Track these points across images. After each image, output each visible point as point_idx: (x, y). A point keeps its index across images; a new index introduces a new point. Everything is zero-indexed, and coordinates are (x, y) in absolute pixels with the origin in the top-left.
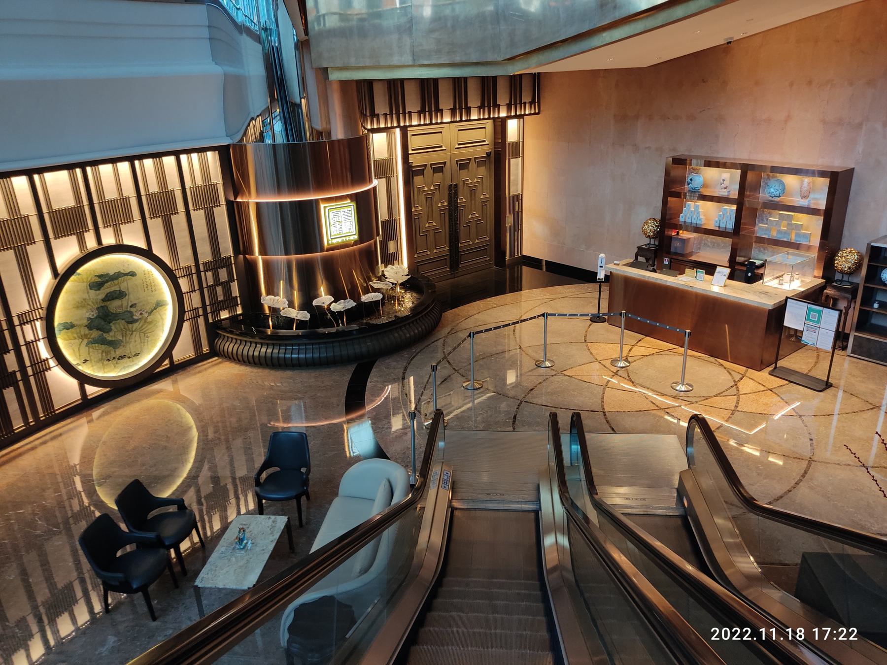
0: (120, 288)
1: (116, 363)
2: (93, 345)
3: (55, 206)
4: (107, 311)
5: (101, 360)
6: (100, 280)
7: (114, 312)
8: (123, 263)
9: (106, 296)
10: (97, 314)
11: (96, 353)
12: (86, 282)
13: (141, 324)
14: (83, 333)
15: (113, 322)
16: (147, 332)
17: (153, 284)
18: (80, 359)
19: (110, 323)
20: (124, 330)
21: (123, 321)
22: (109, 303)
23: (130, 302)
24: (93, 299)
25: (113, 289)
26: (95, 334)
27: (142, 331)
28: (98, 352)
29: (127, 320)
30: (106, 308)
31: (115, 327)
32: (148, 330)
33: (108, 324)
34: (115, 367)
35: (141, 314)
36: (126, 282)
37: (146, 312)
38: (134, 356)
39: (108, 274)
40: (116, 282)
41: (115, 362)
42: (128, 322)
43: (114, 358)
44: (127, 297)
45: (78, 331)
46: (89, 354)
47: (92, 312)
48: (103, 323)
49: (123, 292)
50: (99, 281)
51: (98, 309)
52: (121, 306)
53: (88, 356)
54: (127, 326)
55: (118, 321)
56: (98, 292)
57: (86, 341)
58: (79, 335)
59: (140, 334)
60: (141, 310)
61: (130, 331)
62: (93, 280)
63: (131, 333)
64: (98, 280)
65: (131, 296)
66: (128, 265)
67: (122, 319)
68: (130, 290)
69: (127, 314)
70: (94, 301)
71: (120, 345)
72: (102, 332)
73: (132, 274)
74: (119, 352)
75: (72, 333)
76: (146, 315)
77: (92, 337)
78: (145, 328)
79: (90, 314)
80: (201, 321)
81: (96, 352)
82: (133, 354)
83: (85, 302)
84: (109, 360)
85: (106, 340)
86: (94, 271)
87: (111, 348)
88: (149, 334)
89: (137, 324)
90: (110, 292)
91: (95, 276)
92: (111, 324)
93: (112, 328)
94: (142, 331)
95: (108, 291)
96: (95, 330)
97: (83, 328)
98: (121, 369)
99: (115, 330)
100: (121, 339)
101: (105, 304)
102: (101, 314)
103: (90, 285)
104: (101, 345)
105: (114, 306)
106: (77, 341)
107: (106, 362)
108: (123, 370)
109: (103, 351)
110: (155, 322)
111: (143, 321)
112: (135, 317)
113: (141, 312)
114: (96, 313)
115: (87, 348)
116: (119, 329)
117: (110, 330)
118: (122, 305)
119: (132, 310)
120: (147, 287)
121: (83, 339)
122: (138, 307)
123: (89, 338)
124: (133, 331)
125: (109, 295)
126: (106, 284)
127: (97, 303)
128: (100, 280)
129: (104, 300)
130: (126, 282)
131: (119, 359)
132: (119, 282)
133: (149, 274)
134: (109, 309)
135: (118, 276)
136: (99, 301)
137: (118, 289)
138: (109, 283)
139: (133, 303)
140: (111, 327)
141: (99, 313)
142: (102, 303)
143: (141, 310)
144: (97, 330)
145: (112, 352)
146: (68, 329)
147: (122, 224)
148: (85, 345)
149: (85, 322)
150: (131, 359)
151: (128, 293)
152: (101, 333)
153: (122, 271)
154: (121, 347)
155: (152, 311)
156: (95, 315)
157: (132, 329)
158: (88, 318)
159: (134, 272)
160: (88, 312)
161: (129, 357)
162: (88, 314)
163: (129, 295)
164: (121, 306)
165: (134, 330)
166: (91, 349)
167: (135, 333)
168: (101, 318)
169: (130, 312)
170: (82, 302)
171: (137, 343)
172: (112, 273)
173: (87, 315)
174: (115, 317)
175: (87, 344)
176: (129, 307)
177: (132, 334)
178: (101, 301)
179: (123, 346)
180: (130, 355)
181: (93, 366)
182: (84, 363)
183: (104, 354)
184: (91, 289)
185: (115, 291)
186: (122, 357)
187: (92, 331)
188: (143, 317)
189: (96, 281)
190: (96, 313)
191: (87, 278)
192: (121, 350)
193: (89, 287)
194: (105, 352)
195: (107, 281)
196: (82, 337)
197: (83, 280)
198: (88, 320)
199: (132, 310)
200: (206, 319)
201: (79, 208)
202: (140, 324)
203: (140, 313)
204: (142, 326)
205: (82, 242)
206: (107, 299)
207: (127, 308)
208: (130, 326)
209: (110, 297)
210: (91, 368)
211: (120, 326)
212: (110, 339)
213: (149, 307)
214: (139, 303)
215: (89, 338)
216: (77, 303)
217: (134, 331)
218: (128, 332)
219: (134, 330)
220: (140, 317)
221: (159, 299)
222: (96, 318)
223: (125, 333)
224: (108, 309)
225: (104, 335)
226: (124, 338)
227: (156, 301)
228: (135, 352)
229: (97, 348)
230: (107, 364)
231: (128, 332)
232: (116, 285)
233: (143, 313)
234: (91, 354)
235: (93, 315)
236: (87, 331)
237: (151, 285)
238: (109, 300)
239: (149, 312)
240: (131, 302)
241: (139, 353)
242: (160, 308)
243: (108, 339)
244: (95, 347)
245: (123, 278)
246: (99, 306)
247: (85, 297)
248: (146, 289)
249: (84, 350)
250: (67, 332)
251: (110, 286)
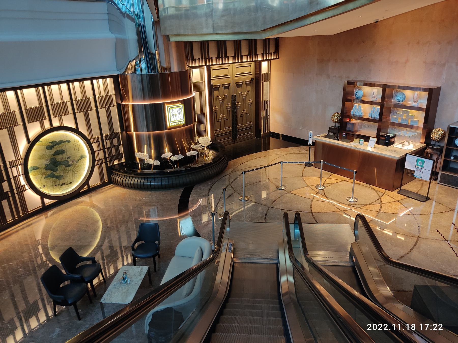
0: (62, 148)
1: (60, 187)
2: (48, 178)
3: (29, 106)
4: (55, 161)
5: (52, 186)
6: (52, 144)
7: (59, 161)
8: (64, 135)
9: (55, 153)
10: (50, 162)
11: (50, 182)
12: (45, 145)
14: (43, 172)
15: (59, 166)
18: (41, 185)
19: (57, 167)
20: (64, 170)
21: (64, 166)
22: (56, 156)
23: (67, 156)
24: (48, 154)
25: (58, 149)
26: (49, 172)
27: (73, 171)
28: (50, 181)
29: (66, 165)
30: (55, 159)
31: (60, 169)
32: (76, 170)
33: (56, 167)
34: (59, 189)
35: (73, 162)
36: (65, 146)
37: (76, 161)
38: (69, 184)
39: (56, 141)
40: (60, 145)
41: (59, 187)
43: (59, 185)
44: (65, 153)
45: (40, 171)
46: (46, 183)
47: (48, 161)
48: (53, 167)
49: (64, 150)
50: (51, 145)
51: (50, 159)
52: (63, 158)
53: (45, 183)
54: (66, 168)
55: (61, 166)
56: (50, 151)
57: (44, 176)
58: (41, 173)
59: (72, 172)
60: (73, 160)
61: (67, 171)
62: (48, 145)
63: (68, 172)
64: (51, 144)
65: (68, 153)
67: (63, 165)
68: (67, 149)
69: (66, 162)
70: (49, 155)
72: (53, 171)
74: (62, 181)
75: (37, 172)
76: (75, 163)
77: (47, 174)
78: (75, 169)
79: (47, 162)
81: (50, 182)
82: (69, 183)
83: (44, 156)
84: (56, 186)
85: (55, 175)
86: (48, 140)
87: (57, 180)
89: (71, 167)
90: (57, 151)
91: (49, 142)
92: (57, 167)
93: (58, 169)
94: (73, 171)
95: (56, 150)
96: (49, 170)
97: (43, 169)
98: (62, 191)
99: (60, 170)
100: (63, 175)
101: (54, 157)
102: (52, 162)
103: (47, 147)
104: (52, 178)
105: (59, 158)
106: (40, 176)
107: (55, 187)
108: (63, 191)
109: (53, 181)
112: (70, 164)
113: (73, 161)
114: (50, 162)
115: (45, 179)
116: (62, 170)
117: (57, 170)
118: (63, 157)
119: (68, 160)
121: (43, 175)
122: (71, 158)
123: (46, 174)
124: (68, 171)
125: (56, 152)
126: (55, 147)
127: (50, 156)
128: (52, 144)
129: (53, 155)
130: (65, 146)
131: (61, 185)
132: (62, 145)
134: (56, 159)
135: (61, 142)
136: (51, 155)
138: (56, 146)
139: (69, 156)
140: (57, 168)
141: (51, 162)
142: (53, 156)
143: (73, 160)
144: (50, 170)
145: (58, 182)
146: (35, 170)
147: (63, 116)
148: (44, 178)
149: (44, 166)
151: (66, 151)
152: (52, 172)
153: (63, 140)
154: (63, 179)
155: (79, 160)
156: (49, 163)
157: (68, 170)
158: (45, 164)
159: (69, 140)
160: (45, 161)
162: (45, 162)
163: (67, 152)
164: (63, 158)
165: (69, 170)
166: (47, 180)
167: (69, 172)
168: (52, 164)
169: (67, 161)
171: (71, 177)
172: (58, 141)
173: (45, 163)
174: (60, 163)
175: (45, 178)
176: (67, 158)
177: (68, 172)
180: (67, 183)
181: (48, 189)
182: (43, 187)
183: (54, 183)
184: (47, 149)
185: (59, 150)
186: (63, 184)
187: (47, 171)
188: (74, 163)
189: (50, 145)
190: (50, 162)
191: (45, 143)
192: (62, 181)
193: (46, 148)
194: (54, 182)
195: (55, 145)
196: (43, 174)
198: (45, 165)
199: (68, 160)
200: (107, 165)
201: (41, 107)
202: (72, 167)
203: (72, 161)
204: (73, 168)
206: (55, 154)
207: (66, 159)
208: (67, 168)
209: (57, 153)
210: (47, 190)
211: (62, 168)
212: (57, 175)
215: (46, 174)
216: (40, 156)
217: (69, 171)
218: (66, 171)
219: (69, 170)
220: (72, 163)
221: (82, 154)
222: (50, 164)
223: (65, 172)
224: (56, 160)
225: (54, 173)
226: (64, 174)
227: (80, 155)
229: (50, 180)
230: (55, 188)
231: (66, 171)
232: (60, 147)
233: (74, 161)
234: (47, 182)
235: (48, 163)
236: (45, 171)
238: (56, 155)
239: (77, 161)
240: (68, 156)
241: (72, 182)
243: (56, 175)
244: (49, 179)
245: (63, 143)
246: (51, 158)
247: (44, 153)
248: (75, 149)
249: (44, 180)
250: (35, 171)
251: (57, 147)
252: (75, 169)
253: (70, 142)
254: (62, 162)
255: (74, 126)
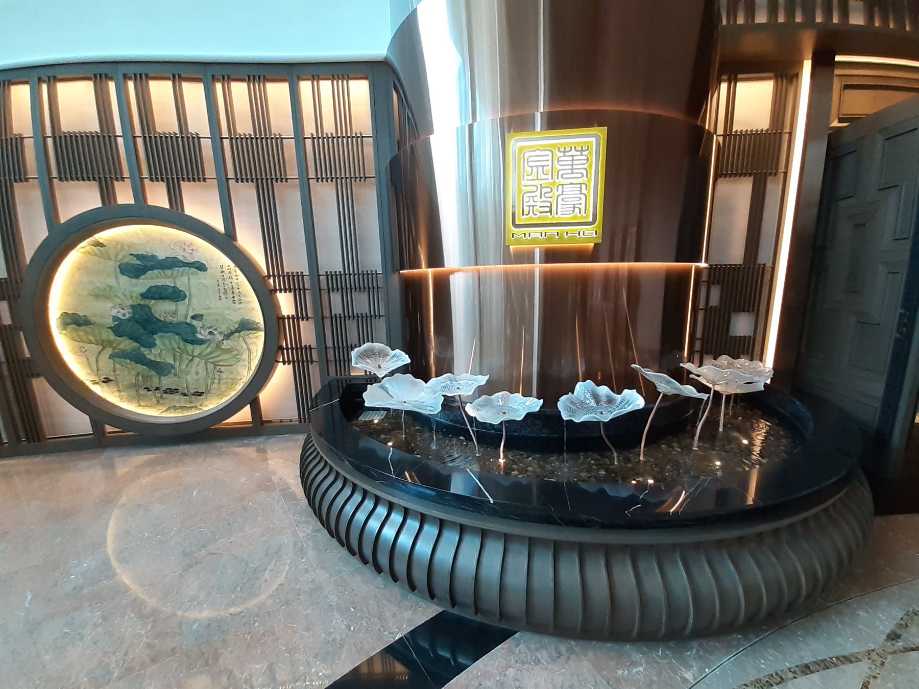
2: (123, 359)
4: (149, 314)
5: (135, 386)
6: (138, 262)
7: (162, 319)
8: (183, 244)
10: (132, 315)
12: (115, 261)
13: (209, 350)
15: (159, 334)
16: (221, 363)
17: (236, 291)
18: (98, 375)
19: (153, 334)
20: (179, 350)
21: (177, 337)
22: (153, 301)
23: (191, 310)
26: (127, 344)
28: (129, 372)
31: (163, 343)
34: (158, 402)
35: (210, 333)
37: (221, 333)
38: (193, 395)
40: (168, 272)
42: (186, 341)
43: (157, 389)
44: (187, 300)
46: (114, 371)
47: (123, 309)
51: (132, 307)
52: (175, 313)
53: (112, 373)
54: (184, 345)
59: (206, 364)
60: (210, 327)
62: (126, 260)
63: (190, 358)
64: (135, 261)
65: (194, 300)
66: (193, 250)
67: (177, 334)
68: (194, 291)
69: (186, 327)
71: (170, 372)
72: (139, 345)
73: (201, 267)
74: (167, 382)
75: (87, 333)
79: (119, 312)
80: (315, 371)
81: (129, 372)
82: (192, 392)
87: (153, 373)
88: (222, 369)
89: (204, 346)
91: (131, 254)
92: (155, 336)
96: (125, 337)
100: (172, 363)
102: (137, 316)
105: (162, 309)
106: (95, 348)
107: (142, 392)
109: (138, 374)
110: (235, 352)
111: (213, 345)
113: (211, 330)
115: (111, 361)
119: (195, 323)
120: (225, 292)
121: (104, 348)
122: (208, 320)
124: (193, 357)
125: (154, 289)
128: (138, 262)
129: (144, 296)
132: (175, 273)
133: (230, 273)
135: (172, 264)
136: (135, 295)
137: (172, 285)
138: (155, 271)
140: (155, 340)
141: (134, 313)
142: (141, 300)
143: (210, 327)
144: (131, 339)
145: (154, 379)
146: (79, 325)
148: (108, 356)
149: (110, 322)
150: (188, 397)
152: (136, 344)
153: (181, 258)
155: (232, 333)
156: (128, 316)
157: (193, 352)
158: (114, 317)
161: (185, 395)
162: (116, 311)
163: (190, 299)
164: (175, 313)
166: (117, 365)
167: (197, 360)
168: (137, 322)
169: (193, 327)
170: (105, 290)
172: (161, 255)
173: (114, 312)
174: (165, 327)
175: (112, 357)
176: (189, 317)
177: (192, 360)
178: (140, 297)
179: (175, 375)
180: (186, 391)
181: (120, 391)
182: (103, 382)
183: (140, 378)
184: (122, 273)
185: (165, 287)
186: (171, 391)
188: (213, 339)
190: (129, 313)
192: (170, 380)
193: (119, 270)
194: (143, 376)
196: (105, 344)
197: (108, 255)
199: (195, 323)
202: (207, 348)
203: (208, 331)
204: (211, 353)
205: (107, 194)
206: (150, 295)
208: (190, 347)
210: (117, 394)
213: (227, 325)
214: (209, 315)
215: (115, 348)
218: (185, 356)
220: (209, 337)
221: (247, 318)
222: (129, 320)
223: (180, 356)
224: (151, 311)
225: (142, 349)
226: (178, 363)
227: (239, 319)
228: (195, 389)
229: (129, 366)
230: (144, 395)
231: (185, 356)
233: (215, 333)
234: (117, 372)
235: (124, 315)
236: (112, 337)
237: (233, 293)
238: (152, 298)
239: (226, 333)
240: (194, 309)
241: (203, 393)
242: (247, 332)
243: (148, 357)
244: (126, 364)
248: (223, 297)
249: (106, 363)
250: (76, 330)
251: (157, 275)
252: (219, 356)
253: (206, 270)
254: (171, 323)
255: (218, 224)
